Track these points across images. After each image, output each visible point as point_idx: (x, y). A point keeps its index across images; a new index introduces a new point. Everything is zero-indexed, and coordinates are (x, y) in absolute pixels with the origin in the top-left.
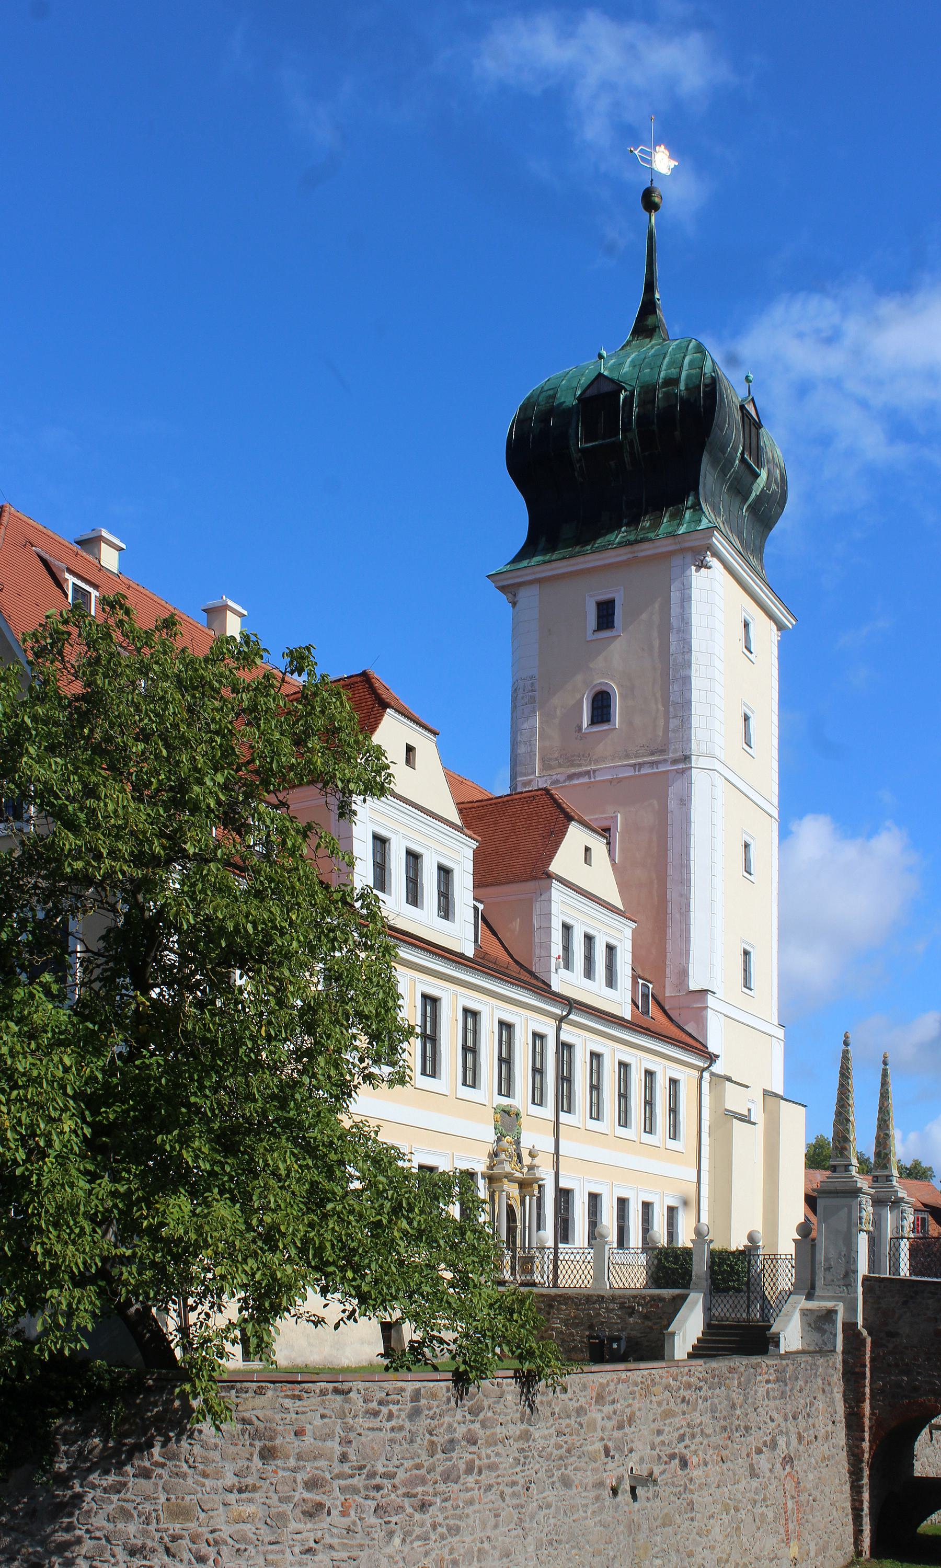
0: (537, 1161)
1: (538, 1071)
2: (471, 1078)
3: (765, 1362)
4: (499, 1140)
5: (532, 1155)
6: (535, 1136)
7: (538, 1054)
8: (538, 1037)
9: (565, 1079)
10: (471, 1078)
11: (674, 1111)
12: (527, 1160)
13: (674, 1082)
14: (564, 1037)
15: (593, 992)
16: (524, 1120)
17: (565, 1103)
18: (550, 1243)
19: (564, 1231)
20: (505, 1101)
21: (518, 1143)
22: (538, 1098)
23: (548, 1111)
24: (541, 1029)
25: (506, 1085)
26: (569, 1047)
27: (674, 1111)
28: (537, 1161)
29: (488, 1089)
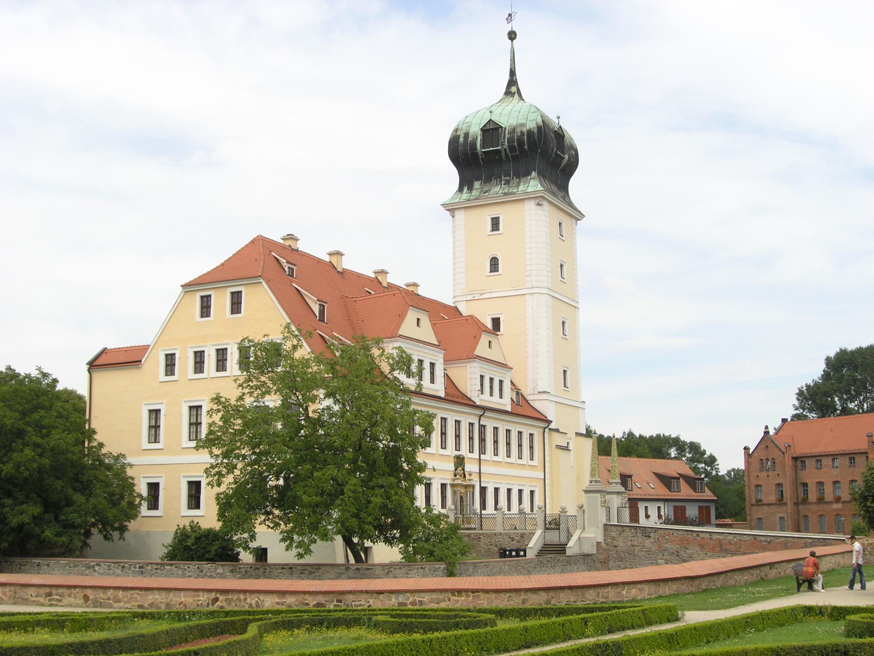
0: (472, 477)
1: (471, 438)
2: (444, 446)
3: (562, 557)
4: (456, 469)
5: (470, 475)
6: (470, 467)
7: (471, 431)
8: (471, 425)
9: (482, 440)
10: (444, 446)
11: (531, 447)
12: (468, 477)
13: (531, 435)
14: (482, 423)
15: (494, 401)
16: (466, 460)
17: (482, 450)
18: (478, 511)
19: (483, 506)
20: (458, 453)
21: (463, 470)
22: (471, 451)
23: (476, 455)
24: (472, 421)
25: (458, 447)
26: (484, 426)
27: (531, 447)
28: (472, 477)
29: (450, 451)
